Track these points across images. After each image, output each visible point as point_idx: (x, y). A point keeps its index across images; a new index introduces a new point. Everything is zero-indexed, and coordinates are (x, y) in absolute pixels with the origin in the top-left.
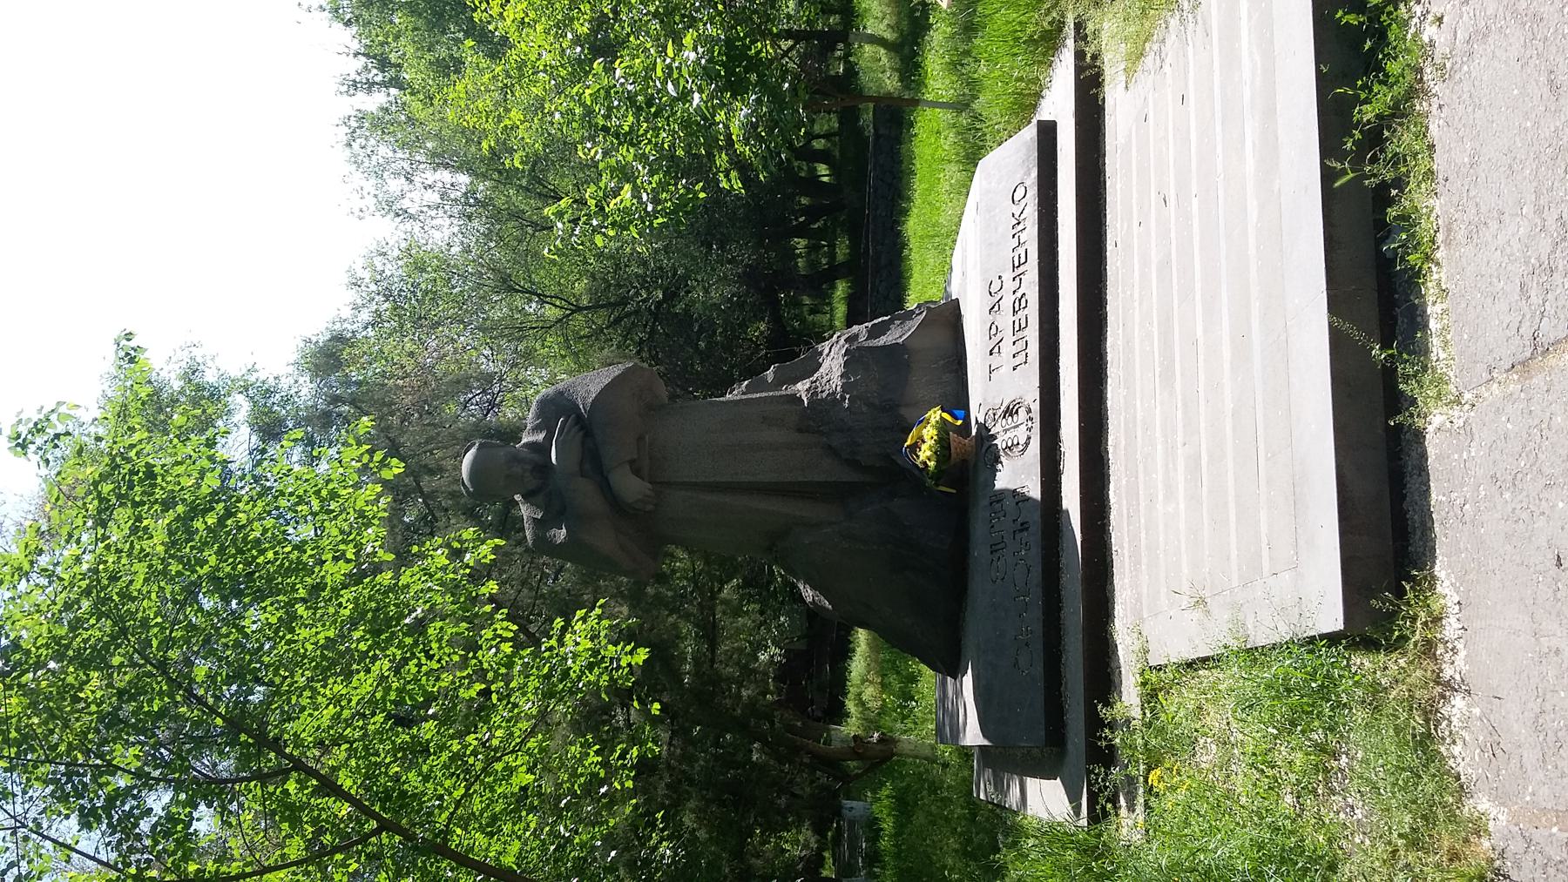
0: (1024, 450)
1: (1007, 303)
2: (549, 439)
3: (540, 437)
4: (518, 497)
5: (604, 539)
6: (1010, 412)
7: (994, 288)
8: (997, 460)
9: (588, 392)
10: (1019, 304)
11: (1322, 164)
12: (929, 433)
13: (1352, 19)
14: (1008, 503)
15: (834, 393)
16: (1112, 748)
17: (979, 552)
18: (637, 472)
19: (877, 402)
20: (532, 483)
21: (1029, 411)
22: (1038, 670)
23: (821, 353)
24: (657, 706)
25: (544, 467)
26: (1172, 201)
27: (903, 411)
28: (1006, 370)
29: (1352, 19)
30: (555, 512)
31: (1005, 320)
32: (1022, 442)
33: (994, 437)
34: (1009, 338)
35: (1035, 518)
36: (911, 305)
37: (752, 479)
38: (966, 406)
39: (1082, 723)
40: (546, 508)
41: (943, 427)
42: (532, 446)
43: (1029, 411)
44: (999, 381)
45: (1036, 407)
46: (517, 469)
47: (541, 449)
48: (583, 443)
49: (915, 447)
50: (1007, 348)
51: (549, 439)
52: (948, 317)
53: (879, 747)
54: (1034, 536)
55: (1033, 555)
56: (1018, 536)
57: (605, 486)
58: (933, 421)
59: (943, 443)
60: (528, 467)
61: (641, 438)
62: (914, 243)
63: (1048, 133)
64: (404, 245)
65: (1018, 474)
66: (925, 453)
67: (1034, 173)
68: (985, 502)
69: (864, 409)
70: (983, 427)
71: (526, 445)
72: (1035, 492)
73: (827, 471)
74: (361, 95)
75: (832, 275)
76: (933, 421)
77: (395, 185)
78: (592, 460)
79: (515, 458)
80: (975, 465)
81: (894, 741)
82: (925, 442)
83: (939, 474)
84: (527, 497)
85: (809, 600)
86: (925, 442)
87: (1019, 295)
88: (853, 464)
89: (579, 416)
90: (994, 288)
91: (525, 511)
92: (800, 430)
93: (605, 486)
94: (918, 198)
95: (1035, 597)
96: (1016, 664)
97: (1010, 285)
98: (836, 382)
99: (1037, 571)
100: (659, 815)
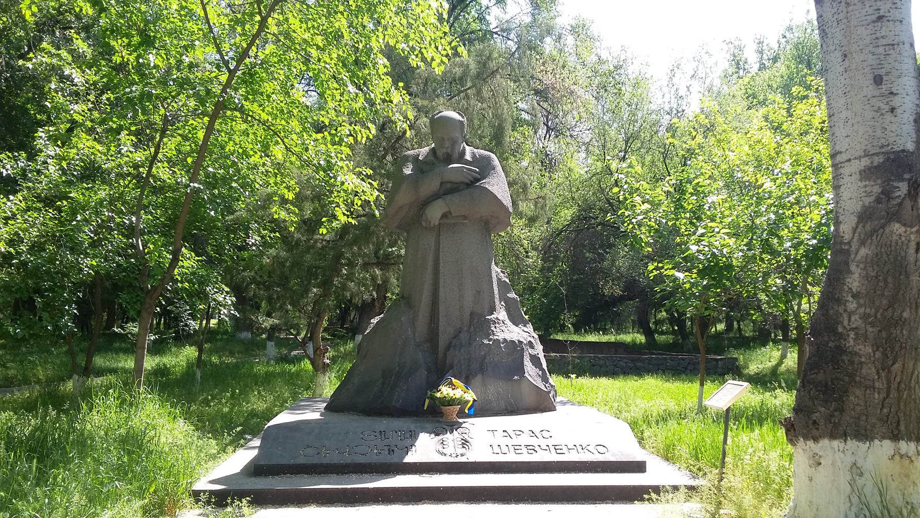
0: (439, 452)
1: (533, 441)
3: (468, 157)
4: (433, 145)
5: (405, 197)
6: (465, 443)
7: (545, 434)
8: (437, 435)
9: (493, 185)
10: (531, 449)
14: (409, 441)
15: (494, 335)
16: (226, 505)
17: (384, 423)
18: (445, 216)
20: (440, 153)
21: (462, 455)
22: (302, 460)
24: (325, 231)
25: (449, 159)
30: (422, 167)
31: (525, 439)
32: (445, 451)
33: (452, 432)
34: (510, 442)
35: (394, 459)
36: (554, 380)
37: (441, 284)
38: (475, 415)
39: (259, 487)
40: (424, 162)
41: (461, 402)
42: (463, 153)
43: (462, 455)
45: (463, 459)
46: (447, 144)
47: (461, 157)
48: (462, 183)
49: (451, 384)
53: (320, 362)
56: (386, 448)
57: (436, 196)
59: (451, 402)
60: (449, 151)
61: (465, 217)
62: (641, 381)
64: (648, 76)
65: (426, 447)
66: (445, 391)
68: (412, 428)
69: (483, 353)
70: (459, 425)
72: (410, 458)
73: (446, 332)
74: (755, 47)
75: (648, 333)
77: (689, 68)
78: (451, 189)
79: (454, 143)
80: (439, 422)
81: (324, 373)
82: (453, 390)
83: (433, 398)
84: (433, 151)
85: (372, 321)
86: (453, 390)
87: (537, 448)
88: (448, 348)
89: (479, 180)
90: (545, 434)
91: (425, 151)
92: (472, 314)
93: (436, 196)
94: (668, 385)
95: (347, 459)
98: (500, 336)
99: (361, 460)
100: (277, 234)
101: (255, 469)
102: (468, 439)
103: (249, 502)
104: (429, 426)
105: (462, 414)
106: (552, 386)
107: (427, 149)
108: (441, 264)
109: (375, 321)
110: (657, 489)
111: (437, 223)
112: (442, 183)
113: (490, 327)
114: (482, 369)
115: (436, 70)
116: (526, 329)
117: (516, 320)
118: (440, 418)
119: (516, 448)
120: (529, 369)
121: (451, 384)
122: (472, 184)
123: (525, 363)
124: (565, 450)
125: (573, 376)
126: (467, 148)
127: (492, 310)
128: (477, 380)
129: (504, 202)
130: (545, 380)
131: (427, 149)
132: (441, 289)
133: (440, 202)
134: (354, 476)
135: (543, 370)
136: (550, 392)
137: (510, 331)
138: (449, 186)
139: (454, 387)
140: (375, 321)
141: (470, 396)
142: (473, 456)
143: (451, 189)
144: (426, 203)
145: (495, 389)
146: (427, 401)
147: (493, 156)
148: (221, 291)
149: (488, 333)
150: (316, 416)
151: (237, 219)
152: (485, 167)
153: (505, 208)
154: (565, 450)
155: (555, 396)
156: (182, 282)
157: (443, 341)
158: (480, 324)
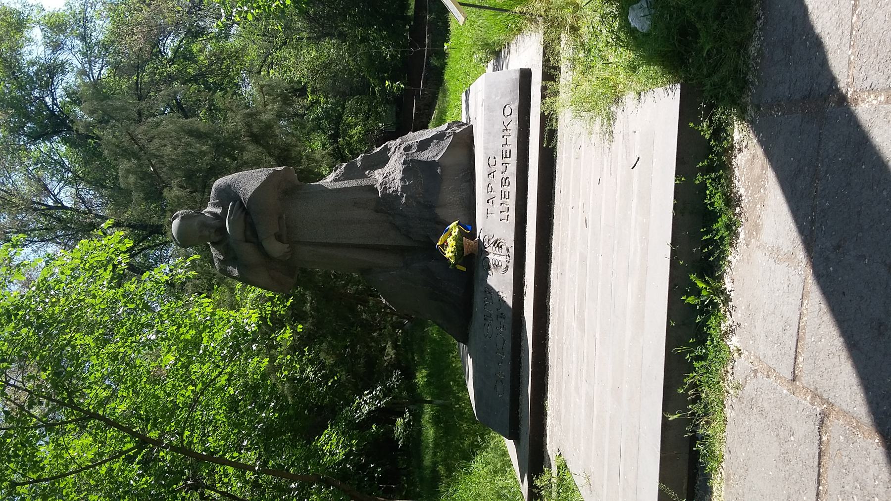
1: (499, 176)
2: (224, 212)
3: (219, 211)
6: (497, 244)
7: (492, 161)
10: (504, 181)
11: (663, 416)
12: (451, 242)
13: (691, 300)
15: (397, 191)
18: (279, 238)
19: (422, 201)
20: (217, 239)
21: (508, 251)
22: (507, 399)
23: (389, 150)
26: (589, 223)
27: (438, 211)
28: (495, 217)
29: (691, 300)
30: (231, 258)
31: (497, 187)
34: (497, 201)
35: (509, 315)
39: (527, 445)
41: (459, 240)
43: (508, 251)
44: (493, 222)
45: (512, 250)
46: (206, 233)
47: (220, 218)
50: (497, 201)
51: (224, 212)
52: (465, 140)
54: (508, 321)
55: (505, 333)
58: (454, 234)
59: (459, 248)
60: (213, 230)
61: (280, 218)
63: (525, 76)
65: (500, 281)
66: (449, 253)
67: (517, 104)
68: (482, 289)
70: (481, 244)
71: (209, 212)
72: (510, 302)
76: (454, 234)
78: (251, 233)
79: (204, 224)
84: (214, 244)
92: (377, 211)
93: (259, 246)
95: (506, 356)
96: (495, 388)
97: (499, 167)
98: (397, 184)
99: (508, 345)
101: (514, 435)
102: (494, 239)
103: (537, 478)
104: (481, 273)
105: (472, 235)
106: (449, 128)
107: (212, 249)
108: (328, 241)
109: (384, 301)
110: (546, 62)
111: (288, 245)
112: (246, 241)
113: (389, 194)
114: (431, 207)
115: (128, 246)
116: (393, 150)
117: (382, 160)
118: (474, 258)
119: (505, 196)
120: (431, 155)
121: (442, 246)
122: (246, 211)
123: (425, 158)
124: (507, 148)
125: (446, 45)
126: (209, 209)
127: (372, 189)
128: (441, 213)
129: (264, 178)
130: (440, 137)
131: (212, 249)
132: (352, 242)
133: (265, 244)
134: (522, 355)
135: (433, 137)
136: (455, 134)
137: (391, 174)
138: (248, 233)
139: (445, 245)
140: (384, 301)
141: (454, 228)
142: (509, 241)
143: (251, 233)
144: (266, 255)
145: (449, 195)
146: (459, 267)
147: (216, 184)
148: (358, 407)
149: (395, 197)
150: (470, 361)
151: (291, 392)
152: (228, 195)
153: (270, 177)
154: (507, 148)
155: (459, 124)
156: (352, 445)
157: (402, 242)
158: (385, 203)
